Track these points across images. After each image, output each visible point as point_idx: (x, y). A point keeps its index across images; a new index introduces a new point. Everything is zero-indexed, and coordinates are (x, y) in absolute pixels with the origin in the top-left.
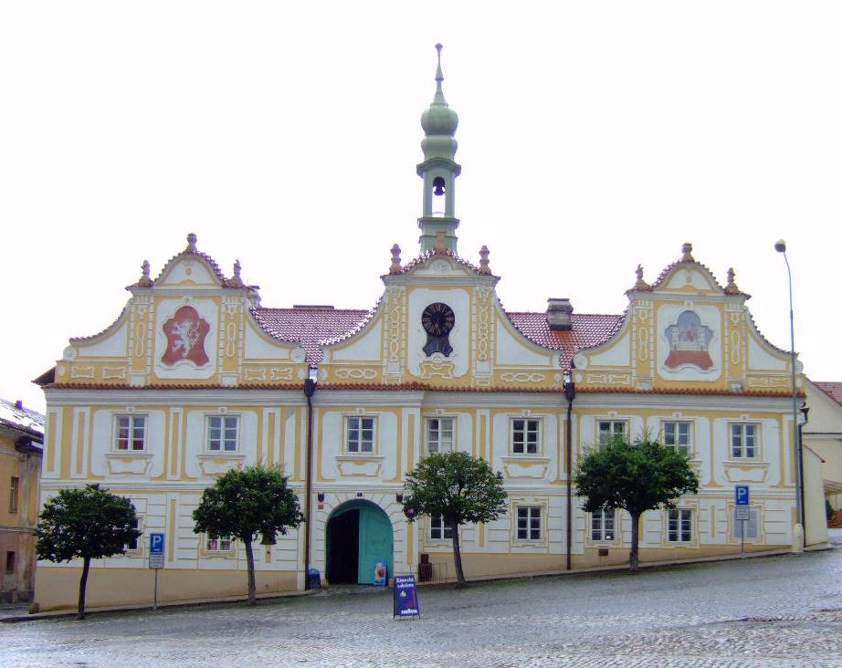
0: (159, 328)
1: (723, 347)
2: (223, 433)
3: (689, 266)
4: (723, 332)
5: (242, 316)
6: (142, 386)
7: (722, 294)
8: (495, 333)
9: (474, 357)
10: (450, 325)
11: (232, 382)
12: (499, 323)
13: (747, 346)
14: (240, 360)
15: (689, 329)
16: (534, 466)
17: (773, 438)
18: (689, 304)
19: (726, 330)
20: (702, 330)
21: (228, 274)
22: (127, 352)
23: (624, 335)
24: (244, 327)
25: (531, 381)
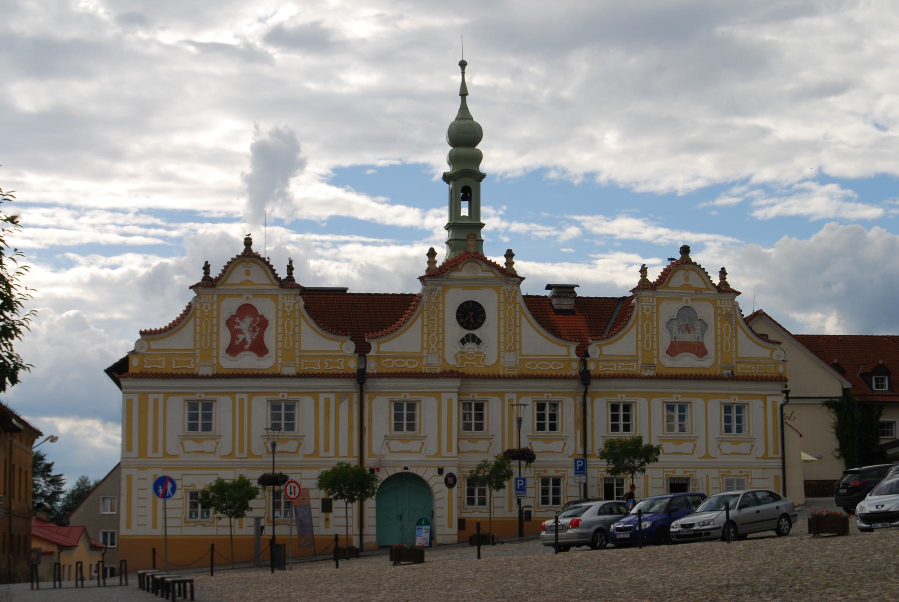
0: (223, 323)
1: (716, 339)
2: (283, 417)
3: (687, 267)
4: (716, 325)
5: (297, 313)
6: (210, 374)
7: (716, 292)
8: (520, 326)
9: (502, 348)
10: (481, 321)
11: (292, 371)
12: (523, 319)
13: (736, 337)
14: (297, 351)
15: (687, 322)
16: (555, 443)
17: (759, 415)
18: (687, 301)
19: (719, 323)
20: (698, 323)
21: (283, 275)
22: (195, 345)
23: (631, 328)
24: (300, 322)
25: (550, 368)
